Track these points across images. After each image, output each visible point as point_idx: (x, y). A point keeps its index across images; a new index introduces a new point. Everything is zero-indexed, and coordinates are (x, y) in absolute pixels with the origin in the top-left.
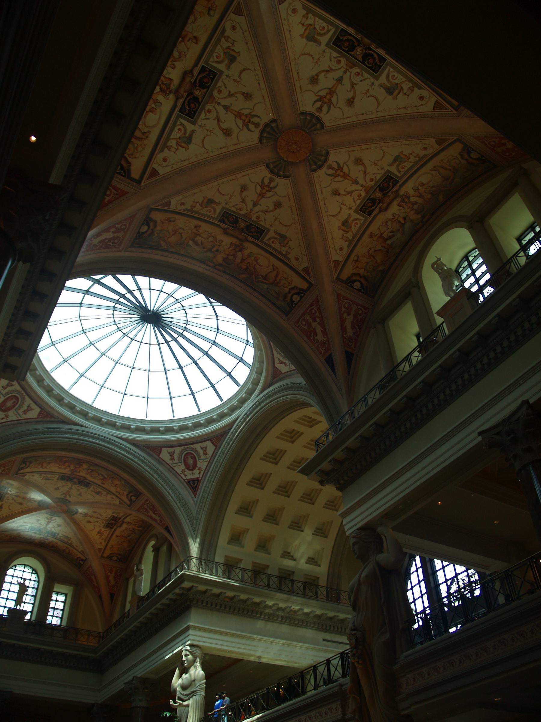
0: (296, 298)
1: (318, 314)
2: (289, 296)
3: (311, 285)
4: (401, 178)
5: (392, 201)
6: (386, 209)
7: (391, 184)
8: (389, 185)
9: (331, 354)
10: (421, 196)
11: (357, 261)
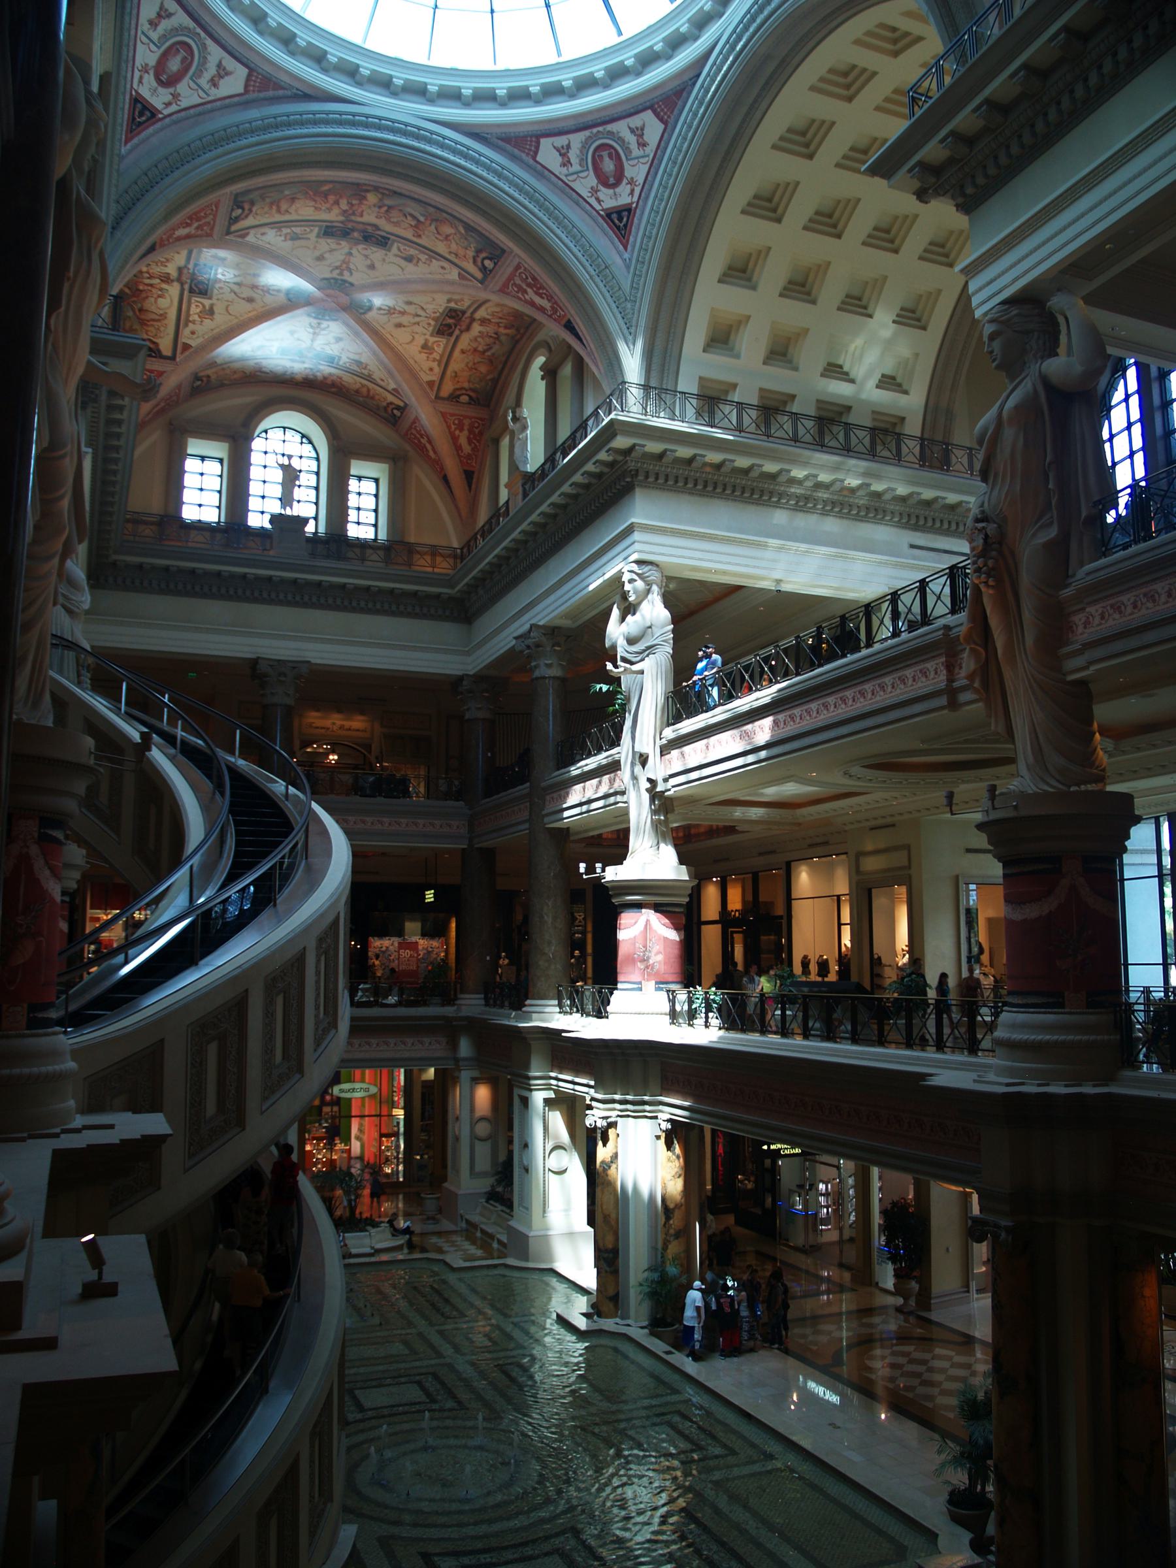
3: (173, 358)
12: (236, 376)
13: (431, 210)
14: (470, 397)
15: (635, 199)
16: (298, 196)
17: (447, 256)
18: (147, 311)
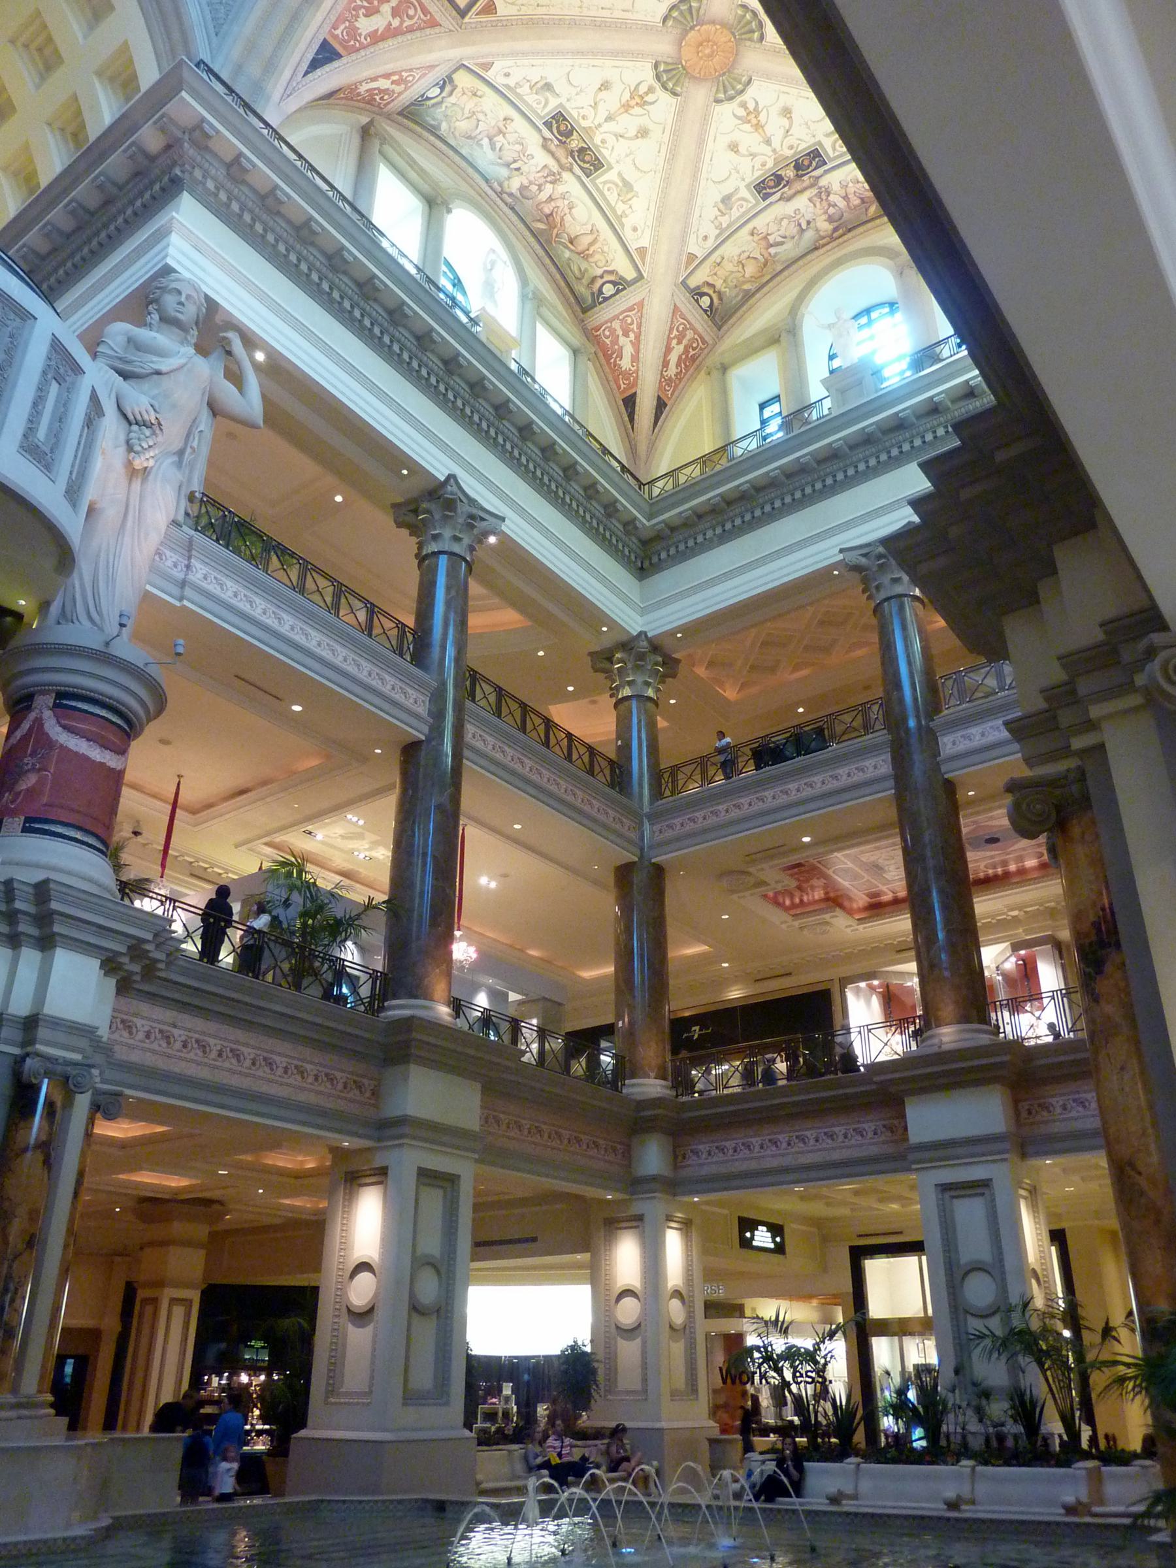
0: (608, 290)
1: (634, 326)
2: (600, 282)
3: (640, 277)
4: (831, 160)
5: (805, 189)
6: (789, 199)
7: (814, 164)
8: (810, 165)
9: (635, 394)
10: (846, 198)
11: (719, 264)
12: (750, 270)
18: (576, 237)
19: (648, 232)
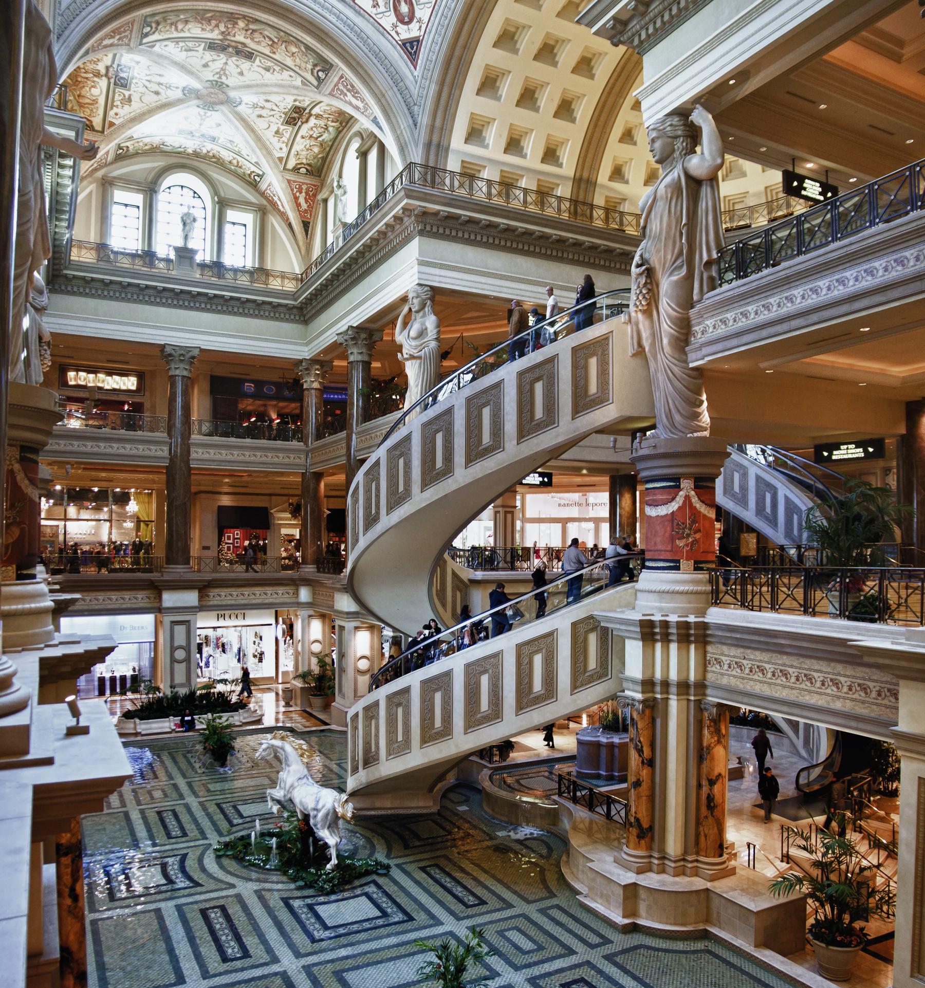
3: (103, 132)
12: (147, 147)
13: (282, 34)
14: (307, 170)
15: (422, 33)
16: (190, 19)
17: (293, 67)
19: (122, 120)
